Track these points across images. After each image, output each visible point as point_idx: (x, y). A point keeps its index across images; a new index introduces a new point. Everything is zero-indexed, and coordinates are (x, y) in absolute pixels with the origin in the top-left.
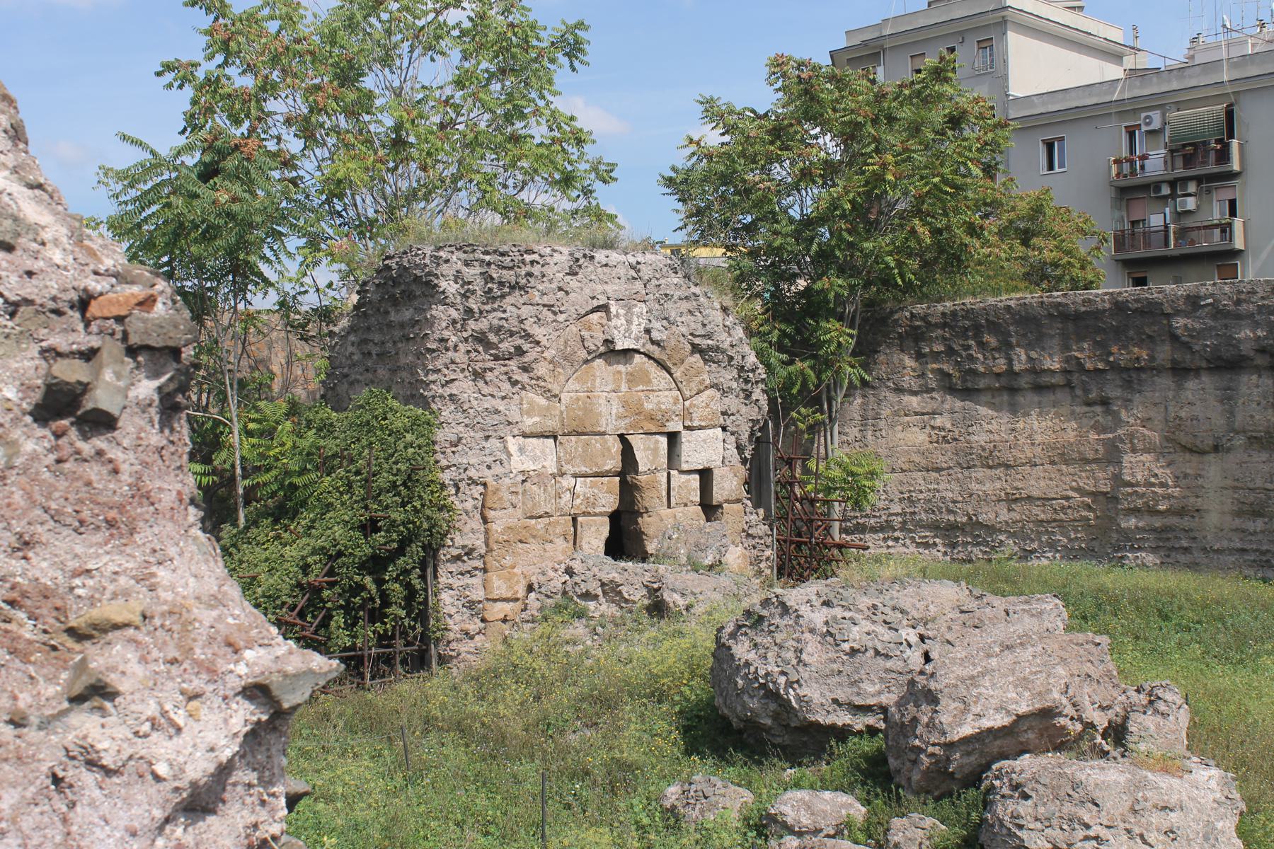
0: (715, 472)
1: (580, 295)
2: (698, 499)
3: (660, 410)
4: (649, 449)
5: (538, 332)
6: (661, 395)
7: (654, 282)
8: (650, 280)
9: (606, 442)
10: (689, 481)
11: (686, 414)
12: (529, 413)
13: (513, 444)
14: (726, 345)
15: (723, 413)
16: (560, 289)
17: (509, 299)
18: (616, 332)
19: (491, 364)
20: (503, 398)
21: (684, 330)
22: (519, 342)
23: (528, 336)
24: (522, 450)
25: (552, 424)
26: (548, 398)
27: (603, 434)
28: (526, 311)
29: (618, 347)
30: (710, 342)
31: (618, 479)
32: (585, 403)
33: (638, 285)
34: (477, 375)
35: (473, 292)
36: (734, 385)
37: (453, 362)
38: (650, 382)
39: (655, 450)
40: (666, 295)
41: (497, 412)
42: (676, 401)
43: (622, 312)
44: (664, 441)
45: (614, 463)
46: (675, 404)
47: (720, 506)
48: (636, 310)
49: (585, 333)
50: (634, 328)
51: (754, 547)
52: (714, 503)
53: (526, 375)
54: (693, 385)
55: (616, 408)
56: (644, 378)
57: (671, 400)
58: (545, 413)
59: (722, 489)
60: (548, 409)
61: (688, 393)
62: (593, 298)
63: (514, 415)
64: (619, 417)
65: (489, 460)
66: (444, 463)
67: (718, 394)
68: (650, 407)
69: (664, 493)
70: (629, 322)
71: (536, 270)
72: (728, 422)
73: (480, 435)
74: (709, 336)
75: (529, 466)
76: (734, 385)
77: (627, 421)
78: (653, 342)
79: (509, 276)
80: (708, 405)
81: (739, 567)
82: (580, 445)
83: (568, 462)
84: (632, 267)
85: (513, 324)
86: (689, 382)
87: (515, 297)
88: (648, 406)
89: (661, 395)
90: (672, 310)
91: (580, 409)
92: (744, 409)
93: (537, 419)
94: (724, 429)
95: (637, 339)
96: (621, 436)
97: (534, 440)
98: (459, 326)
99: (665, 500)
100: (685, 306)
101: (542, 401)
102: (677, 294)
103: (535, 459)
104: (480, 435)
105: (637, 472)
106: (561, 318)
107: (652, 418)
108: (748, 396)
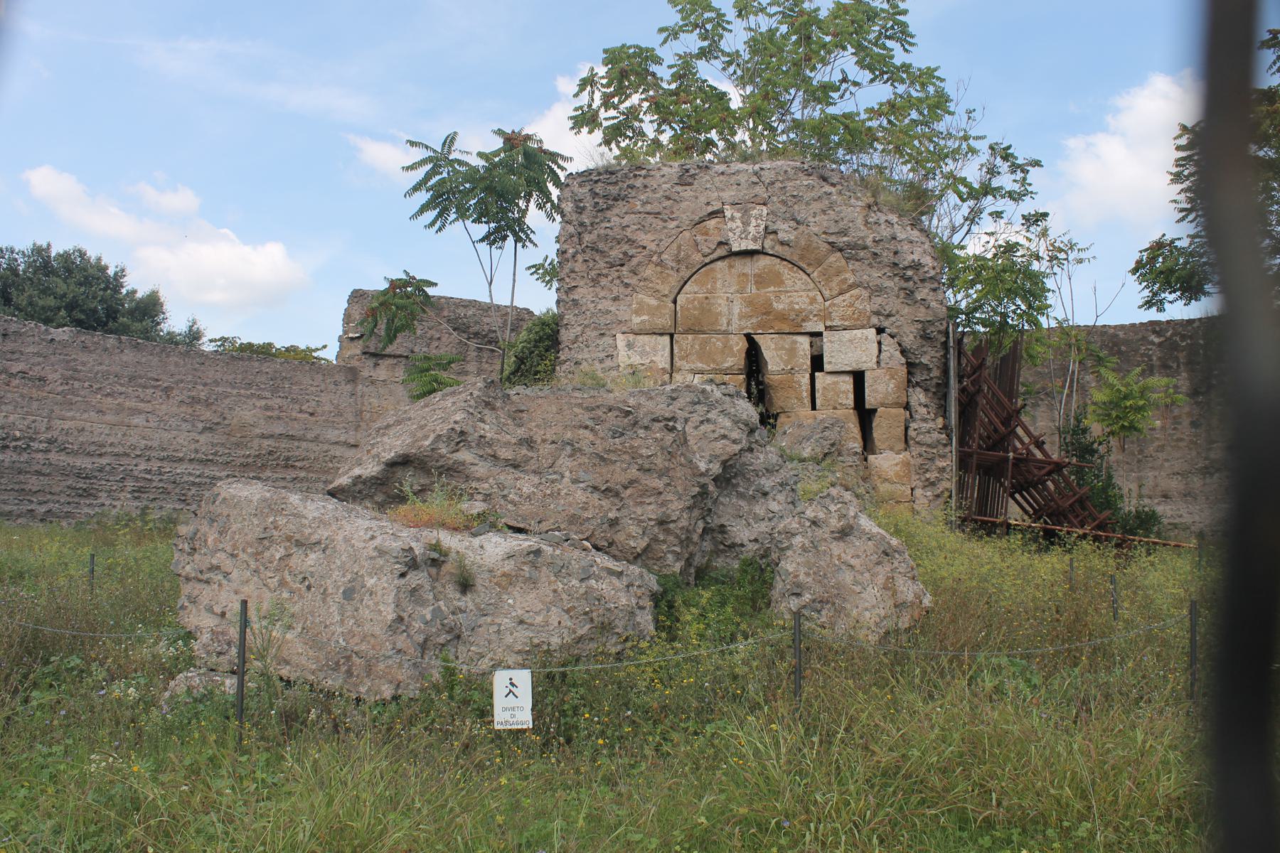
0: (867, 375)
1: (692, 202)
2: (850, 400)
3: (793, 309)
4: (782, 348)
5: (643, 238)
6: (796, 293)
7: (778, 185)
8: (773, 183)
9: (728, 341)
10: (835, 383)
11: (825, 315)
12: (637, 313)
13: (621, 340)
14: (869, 242)
15: (877, 313)
16: (668, 198)
17: (615, 211)
18: (730, 234)
19: (604, 272)
20: (616, 299)
21: (816, 229)
22: (626, 247)
23: (631, 242)
24: (630, 346)
25: (665, 321)
26: (658, 299)
27: (726, 333)
28: (628, 219)
29: (735, 248)
30: (845, 239)
31: (742, 377)
32: (701, 303)
33: (760, 190)
34: (595, 282)
35: (584, 208)
36: (888, 283)
37: (573, 271)
38: (782, 282)
39: (792, 351)
40: (794, 196)
41: (608, 312)
42: (813, 301)
43: (738, 215)
44: (804, 342)
45: (735, 358)
46: (811, 304)
47: (875, 411)
48: (754, 212)
49: (699, 238)
50: (751, 229)
51: (921, 455)
52: (867, 406)
53: (636, 278)
54: (834, 284)
55: (736, 310)
56: (777, 280)
57: (807, 300)
58: (652, 311)
59: (876, 391)
60: (658, 307)
61: (827, 293)
62: (708, 204)
63: (623, 316)
64: (741, 317)
65: (602, 355)
66: (563, 358)
67: (865, 294)
68: (781, 307)
69: (806, 394)
70: (746, 224)
71: (639, 183)
72: (886, 324)
73: (595, 333)
74: (844, 233)
75: (636, 360)
76: (888, 283)
77: (754, 320)
78: (782, 243)
79: (614, 190)
80: (852, 305)
81: (897, 475)
82: (698, 342)
83: (682, 358)
84: (756, 174)
85: (616, 233)
86: (828, 280)
87: (621, 207)
88: (779, 306)
89: (796, 293)
90: (802, 212)
91: (695, 309)
92: (906, 310)
93: (645, 317)
94: (880, 331)
95: (755, 240)
96: (749, 337)
97: (646, 338)
98: (575, 239)
99: (807, 401)
100: (816, 206)
101: (653, 302)
102: (808, 196)
103: (643, 354)
104: (595, 333)
105: (487, 309)
106: (673, 224)
107: (782, 317)
108: (910, 294)
